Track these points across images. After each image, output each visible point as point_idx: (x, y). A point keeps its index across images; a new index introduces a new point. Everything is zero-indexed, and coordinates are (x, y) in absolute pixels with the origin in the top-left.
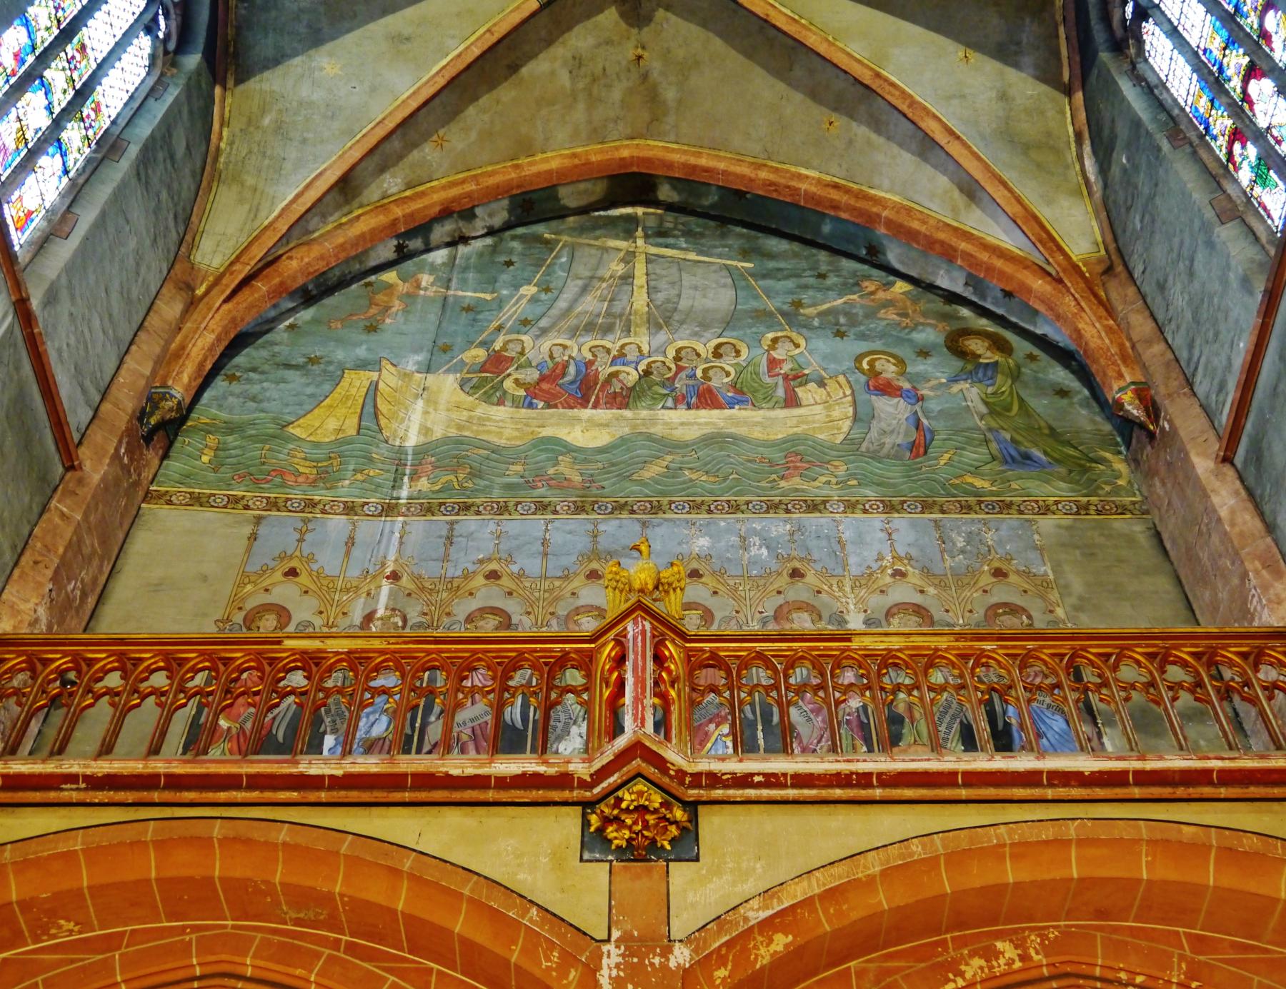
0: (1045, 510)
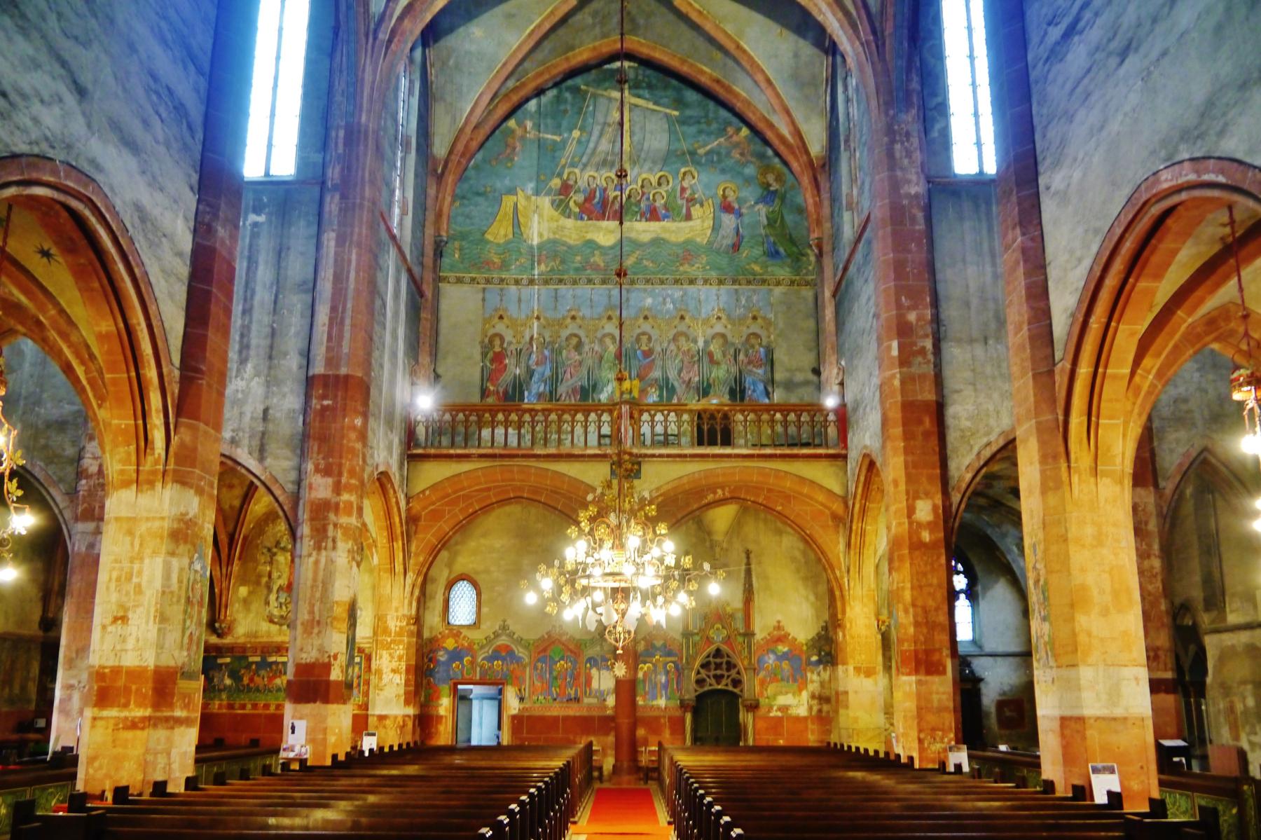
0: (778, 283)
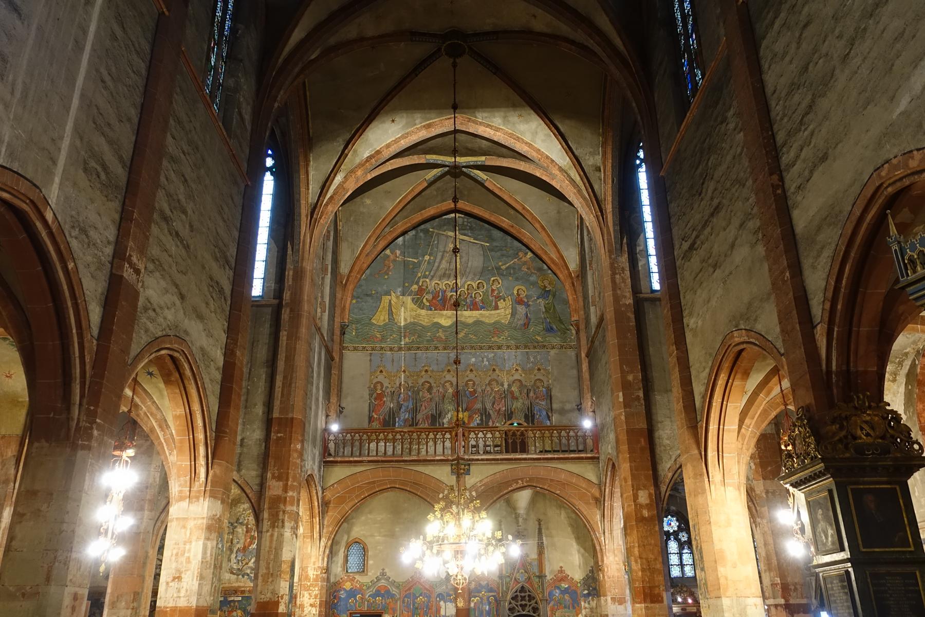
0: (553, 348)
